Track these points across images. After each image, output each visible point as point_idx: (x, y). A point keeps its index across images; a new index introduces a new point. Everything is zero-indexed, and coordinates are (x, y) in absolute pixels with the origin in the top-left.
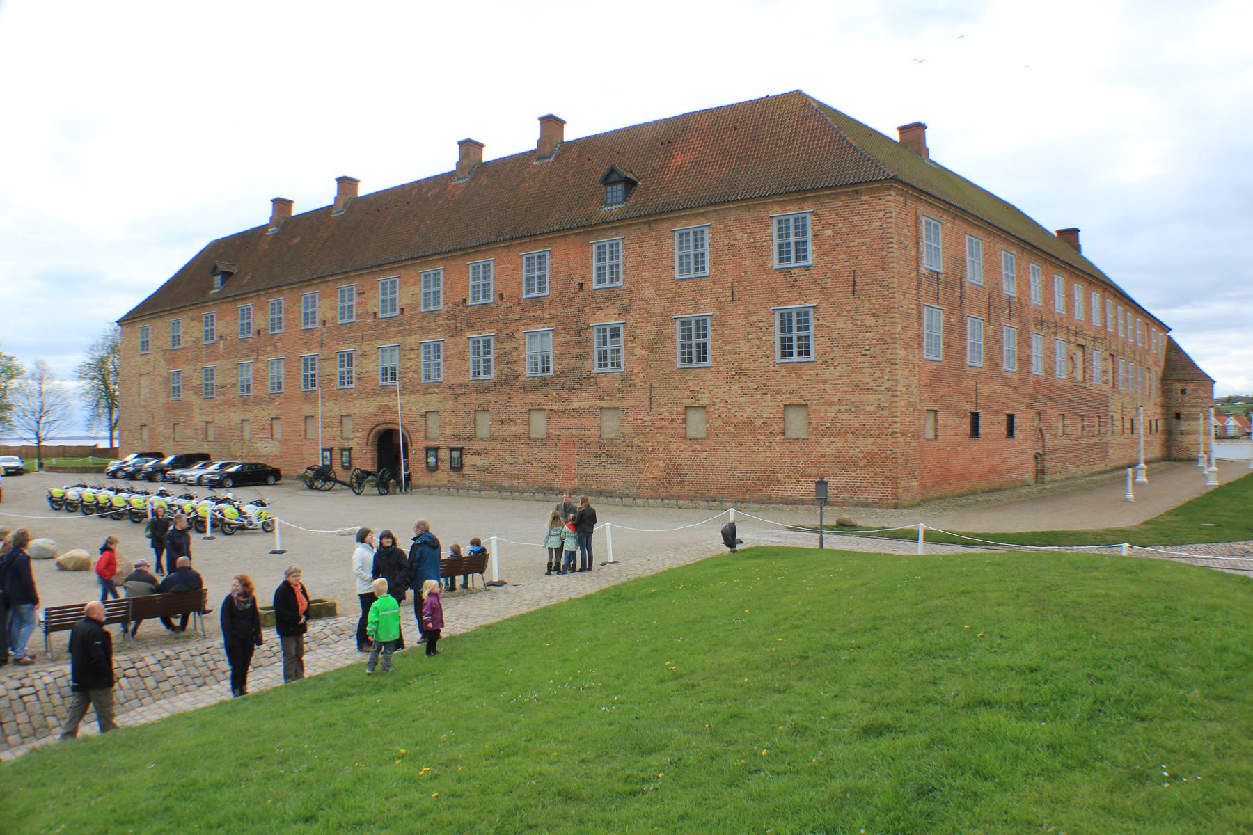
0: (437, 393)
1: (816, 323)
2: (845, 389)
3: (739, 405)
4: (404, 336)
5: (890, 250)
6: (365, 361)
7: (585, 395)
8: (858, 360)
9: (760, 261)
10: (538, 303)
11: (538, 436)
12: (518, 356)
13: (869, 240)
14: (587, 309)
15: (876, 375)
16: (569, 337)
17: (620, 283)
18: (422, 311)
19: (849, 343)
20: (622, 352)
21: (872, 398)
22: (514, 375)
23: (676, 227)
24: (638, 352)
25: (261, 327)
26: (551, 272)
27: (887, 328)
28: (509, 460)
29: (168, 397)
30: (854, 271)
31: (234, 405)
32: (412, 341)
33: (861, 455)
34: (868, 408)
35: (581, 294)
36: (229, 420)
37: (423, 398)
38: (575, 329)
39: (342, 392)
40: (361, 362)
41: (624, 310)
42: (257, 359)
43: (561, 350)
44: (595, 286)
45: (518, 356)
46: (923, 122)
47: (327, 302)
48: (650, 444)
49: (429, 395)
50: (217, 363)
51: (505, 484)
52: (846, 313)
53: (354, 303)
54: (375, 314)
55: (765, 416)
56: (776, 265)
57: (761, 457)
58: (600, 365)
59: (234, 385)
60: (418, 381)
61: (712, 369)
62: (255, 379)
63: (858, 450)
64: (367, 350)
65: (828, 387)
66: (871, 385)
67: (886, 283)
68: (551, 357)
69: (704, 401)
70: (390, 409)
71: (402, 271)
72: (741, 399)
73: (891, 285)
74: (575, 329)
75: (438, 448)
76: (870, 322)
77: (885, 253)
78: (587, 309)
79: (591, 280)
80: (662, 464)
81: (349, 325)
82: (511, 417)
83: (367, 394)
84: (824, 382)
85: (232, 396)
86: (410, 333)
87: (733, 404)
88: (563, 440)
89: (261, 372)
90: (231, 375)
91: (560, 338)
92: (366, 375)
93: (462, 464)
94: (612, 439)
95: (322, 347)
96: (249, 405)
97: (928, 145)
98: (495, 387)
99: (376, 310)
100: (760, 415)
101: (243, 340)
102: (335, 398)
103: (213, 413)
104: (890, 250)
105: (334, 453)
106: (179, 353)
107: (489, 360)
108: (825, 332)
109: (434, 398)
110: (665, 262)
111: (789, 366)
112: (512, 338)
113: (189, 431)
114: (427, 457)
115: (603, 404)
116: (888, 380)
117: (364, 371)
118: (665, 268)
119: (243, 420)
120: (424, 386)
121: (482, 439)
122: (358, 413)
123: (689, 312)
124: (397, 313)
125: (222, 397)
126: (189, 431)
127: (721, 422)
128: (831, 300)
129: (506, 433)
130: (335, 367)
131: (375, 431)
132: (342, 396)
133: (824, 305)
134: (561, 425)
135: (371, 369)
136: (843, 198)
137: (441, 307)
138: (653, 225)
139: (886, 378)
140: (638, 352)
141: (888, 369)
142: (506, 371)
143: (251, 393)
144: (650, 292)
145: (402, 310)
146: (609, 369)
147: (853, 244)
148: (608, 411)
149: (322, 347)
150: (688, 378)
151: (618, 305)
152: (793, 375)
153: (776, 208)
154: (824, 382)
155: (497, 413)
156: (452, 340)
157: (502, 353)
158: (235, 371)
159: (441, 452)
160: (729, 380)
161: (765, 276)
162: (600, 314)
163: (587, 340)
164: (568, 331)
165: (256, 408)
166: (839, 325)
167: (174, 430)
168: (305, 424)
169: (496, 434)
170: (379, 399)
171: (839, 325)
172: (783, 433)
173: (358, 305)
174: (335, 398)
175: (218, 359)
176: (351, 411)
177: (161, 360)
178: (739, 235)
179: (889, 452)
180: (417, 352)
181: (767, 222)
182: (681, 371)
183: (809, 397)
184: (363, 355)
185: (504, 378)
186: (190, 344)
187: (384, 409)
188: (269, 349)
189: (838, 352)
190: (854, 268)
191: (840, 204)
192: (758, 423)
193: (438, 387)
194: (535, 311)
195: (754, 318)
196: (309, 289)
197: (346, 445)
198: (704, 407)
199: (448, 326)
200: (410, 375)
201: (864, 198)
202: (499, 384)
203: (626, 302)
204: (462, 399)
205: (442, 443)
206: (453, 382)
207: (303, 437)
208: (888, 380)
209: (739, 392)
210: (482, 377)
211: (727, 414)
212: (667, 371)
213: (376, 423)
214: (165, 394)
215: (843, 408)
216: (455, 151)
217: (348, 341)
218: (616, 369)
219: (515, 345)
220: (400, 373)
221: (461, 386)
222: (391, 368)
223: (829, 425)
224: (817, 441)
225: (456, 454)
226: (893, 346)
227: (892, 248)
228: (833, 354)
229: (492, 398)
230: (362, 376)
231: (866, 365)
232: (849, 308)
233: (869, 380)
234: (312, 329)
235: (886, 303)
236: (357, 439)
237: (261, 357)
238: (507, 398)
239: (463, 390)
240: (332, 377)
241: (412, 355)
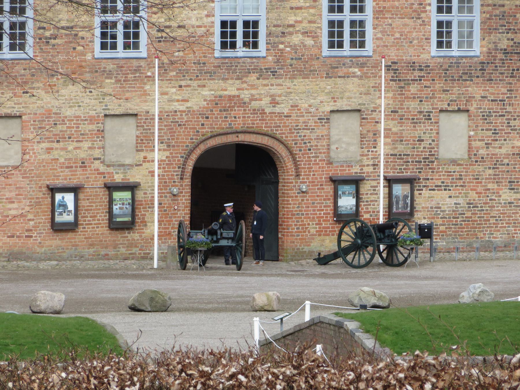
0: (361, 78)
37: (328, 85)
39: (111, 66)
49: (339, 81)
51: (499, 238)
70: (243, 104)
75: (362, 180)
82: (512, 123)
83: (183, 74)
92: (181, 33)
93: (412, 207)
102: (88, 76)
105: (81, 196)
107: (471, 24)
114: (336, 197)
117: (174, 24)
120: (328, 61)
121: (454, 162)
129: (503, 151)
131: (203, 148)
132: (110, 75)
135: (194, 22)
142: (504, 44)
157: (498, 12)
159: (365, 188)
169: (482, 152)
170: (212, 84)
174: (88, 76)
176: (132, 107)
185: (500, 56)
193: (362, 66)
197: (118, 178)
200: (296, 39)
202: (491, 67)
204: (414, 89)
205: (366, 169)
206: (395, 59)
210: (455, 51)
213: (207, 130)
220: (269, 34)
221: (412, 66)
222: (246, 24)
225: (399, 190)
238: (504, 90)
239: (417, 73)
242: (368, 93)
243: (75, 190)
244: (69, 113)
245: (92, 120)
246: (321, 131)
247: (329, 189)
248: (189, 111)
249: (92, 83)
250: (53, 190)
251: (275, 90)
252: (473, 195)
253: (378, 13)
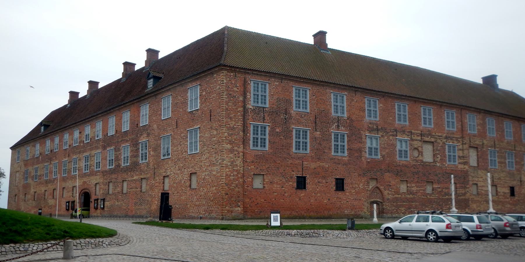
0: (99, 175)
1: (200, 135)
2: (207, 164)
3: (177, 174)
5: (222, 99)
8: (211, 151)
9: (184, 109)
13: (215, 95)
14: (139, 135)
15: (216, 157)
19: (209, 143)
23: (162, 96)
27: (220, 135)
28: (117, 203)
30: (211, 110)
33: (212, 195)
34: (214, 173)
35: (137, 129)
42: (51, 163)
46: (327, 32)
48: (153, 194)
50: (39, 165)
52: (208, 130)
55: (185, 179)
61: (171, 159)
63: (211, 193)
65: (202, 164)
67: (220, 114)
71: (91, 122)
73: (222, 115)
76: (215, 133)
77: (220, 100)
81: (76, 147)
88: (131, 193)
97: (327, 42)
102: (71, 179)
103: (37, 188)
104: (222, 99)
111: (191, 156)
115: (142, 177)
116: (220, 159)
123: (166, 134)
128: (204, 124)
133: (202, 127)
134: (131, 187)
136: (209, 77)
139: (219, 158)
141: (220, 154)
147: (211, 97)
150: (164, 163)
151: (147, 133)
152: (193, 159)
153: (190, 84)
161: (186, 116)
166: (206, 135)
167: (25, 197)
168: (63, 191)
171: (206, 135)
175: (39, 164)
179: (220, 193)
182: (163, 160)
183: (197, 169)
189: (206, 148)
190: (211, 108)
191: (208, 79)
192: (183, 182)
193: (99, 172)
207: (62, 197)
208: (220, 159)
209: (178, 168)
211: (174, 178)
213: (82, 189)
214: (23, 180)
215: (207, 173)
216: (122, 67)
223: (202, 182)
226: (222, 143)
227: (223, 97)
228: (204, 149)
229: (113, 176)
231: (213, 153)
232: (209, 127)
233: (214, 160)
235: (220, 123)
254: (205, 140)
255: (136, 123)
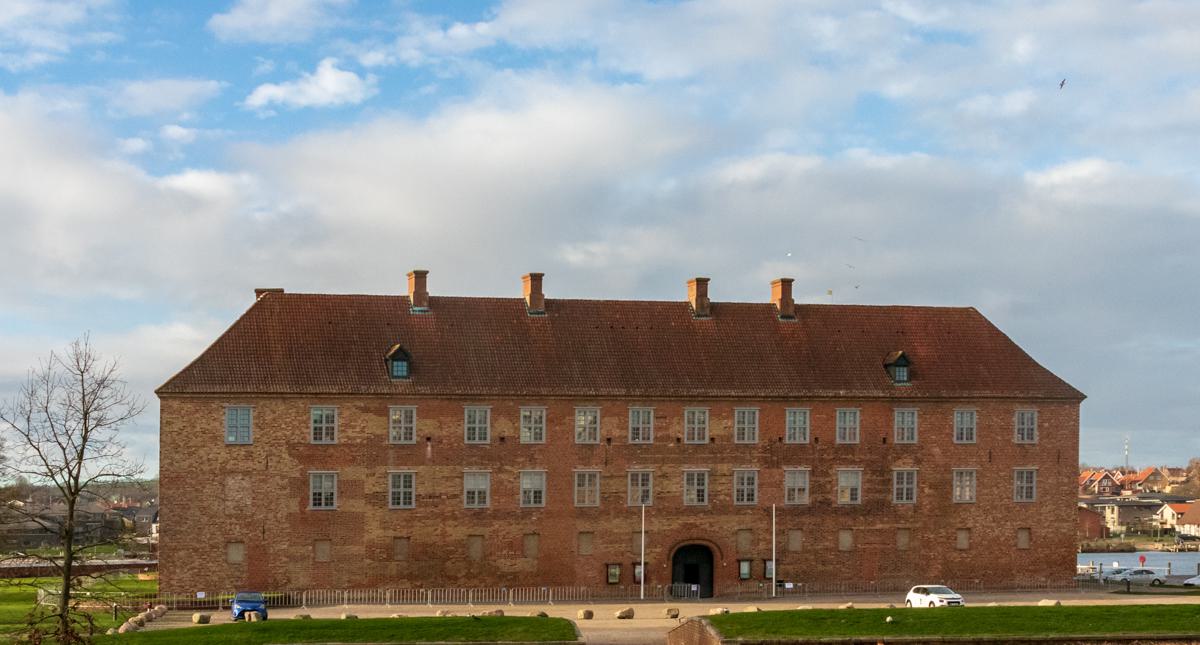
2: (1052, 519)
3: (992, 528)
4: (715, 463)
6: (667, 482)
7: (885, 519)
9: (1007, 438)
10: (849, 449)
11: (845, 549)
12: (831, 488)
16: (875, 477)
17: (915, 441)
18: (736, 442)
20: (915, 491)
21: (1065, 525)
22: (827, 503)
24: (927, 490)
25: (506, 434)
26: (862, 426)
28: (820, 567)
29: (303, 503)
31: (456, 519)
32: (724, 468)
34: (1065, 531)
36: (444, 534)
37: (736, 518)
38: (879, 472)
40: (662, 483)
41: (918, 462)
43: (868, 485)
44: (896, 442)
45: (831, 488)
47: (615, 420)
53: (652, 425)
54: (679, 440)
56: (1015, 441)
57: (1003, 561)
58: (898, 498)
59: (455, 496)
60: (730, 503)
62: (494, 492)
64: (670, 470)
66: (1065, 517)
68: (859, 492)
69: (970, 525)
72: (993, 524)
74: (879, 472)
76: (1066, 480)
78: (890, 457)
79: (893, 436)
80: (939, 566)
81: (645, 447)
84: (1041, 514)
85: (450, 509)
86: (722, 460)
87: (988, 527)
89: (506, 483)
90: (448, 483)
91: (868, 477)
92: (668, 495)
94: (906, 551)
95: (606, 464)
96: (484, 518)
98: (809, 510)
99: (680, 436)
100: (1003, 535)
101: (471, 447)
106: (331, 450)
108: (1042, 485)
109: (748, 518)
110: (947, 431)
112: (826, 474)
113: (355, 549)
115: (900, 526)
118: (947, 434)
119: (470, 536)
121: (796, 552)
122: (656, 530)
124: (707, 441)
125: (429, 510)
126: (355, 549)
127: (980, 539)
130: (626, 485)
134: (866, 541)
137: (757, 441)
138: (940, 404)
140: (927, 490)
143: (488, 504)
144: (937, 450)
145: (712, 439)
146: (905, 501)
148: (903, 532)
149: (606, 464)
153: (1017, 405)
154: (1041, 514)
155: (811, 532)
156: (767, 470)
158: (457, 479)
160: (986, 512)
162: (900, 462)
163: (889, 480)
164: (874, 472)
165: (497, 525)
166: (1050, 481)
171: (1050, 481)
172: (1015, 545)
173: (657, 429)
175: (423, 464)
177: (285, 456)
178: (995, 419)
180: (730, 478)
181: (1011, 413)
184: (664, 476)
185: (818, 504)
186: (358, 441)
187: (687, 526)
188: (521, 460)
192: (1002, 539)
193: (752, 509)
194: (848, 454)
195: (1002, 474)
196: (587, 403)
198: (969, 529)
199: (765, 459)
201: (1067, 406)
203: (919, 455)
212: (946, 504)
217: (644, 461)
218: (909, 502)
219: (830, 479)
220: (709, 495)
224: (1035, 550)
229: (806, 519)
230: (662, 495)
234: (592, 445)
236: (655, 555)
237: (507, 467)
240: (623, 495)
241: (724, 480)
242: (754, 522)
243: (620, 565)
244: (616, 531)
245: (627, 534)
246: (733, 539)
247: (737, 564)
248: (672, 530)
249: (627, 518)
250: (607, 566)
251: (712, 520)
252: (805, 567)
253: (761, 485)
254: (1047, 487)
255: (883, 436)
